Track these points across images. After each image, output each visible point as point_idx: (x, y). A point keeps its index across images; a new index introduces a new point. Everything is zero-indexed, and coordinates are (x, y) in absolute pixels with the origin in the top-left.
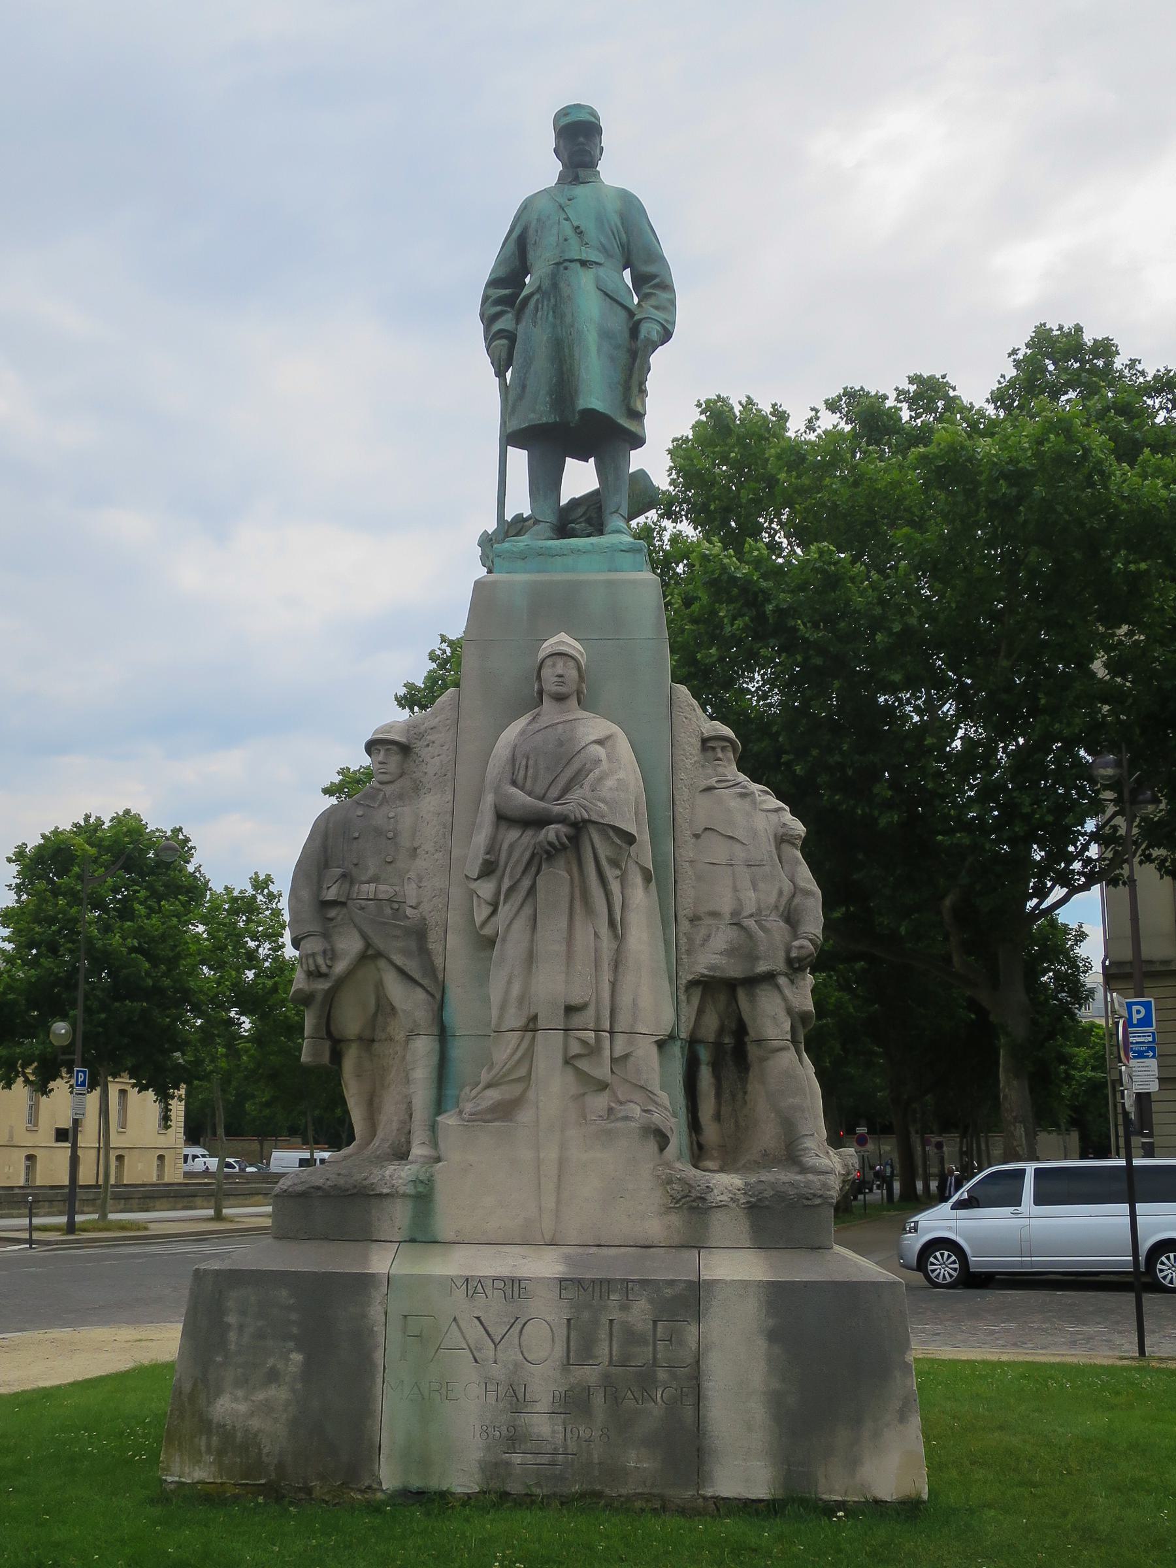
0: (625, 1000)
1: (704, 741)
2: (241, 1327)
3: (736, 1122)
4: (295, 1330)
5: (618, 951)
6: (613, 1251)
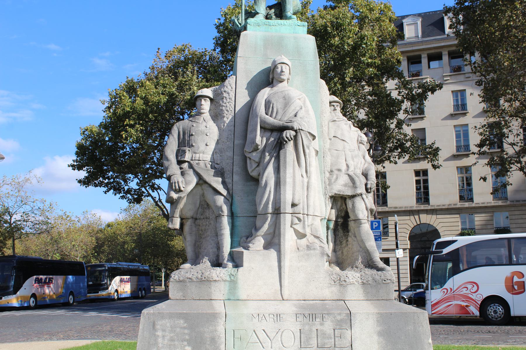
0: (311, 203)
1: (330, 103)
2: (163, 337)
3: (342, 252)
4: (187, 337)
5: (308, 183)
6: (311, 302)
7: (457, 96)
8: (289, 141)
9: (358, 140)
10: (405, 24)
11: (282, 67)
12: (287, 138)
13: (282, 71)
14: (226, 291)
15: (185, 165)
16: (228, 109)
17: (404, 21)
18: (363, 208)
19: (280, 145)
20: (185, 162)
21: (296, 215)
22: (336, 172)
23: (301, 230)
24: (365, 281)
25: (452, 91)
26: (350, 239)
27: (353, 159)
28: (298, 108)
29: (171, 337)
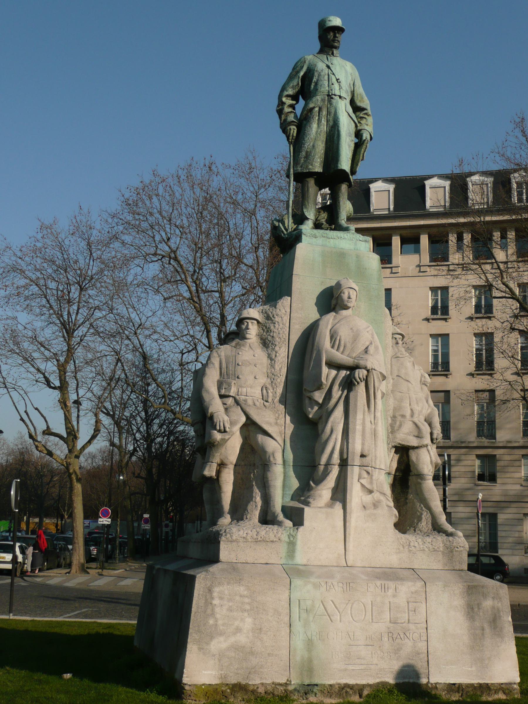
7: (436, 295)
8: (361, 381)
9: (421, 381)
10: (372, 190)
11: (349, 293)
12: (360, 378)
13: (349, 298)
14: (284, 554)
15: (230, 401)
16: (281, 336)
17: (371, 186)
18: (427, 461)
19: (349, 384)
20: (229, 396)
21: (365, 468)
22: (399, 418)
23: (368, 486)
24: (436, 548)
25: (430, 288)
26: (411, 496)
27: (417, 403)
28: (367, 343)
29: (231, 607)
